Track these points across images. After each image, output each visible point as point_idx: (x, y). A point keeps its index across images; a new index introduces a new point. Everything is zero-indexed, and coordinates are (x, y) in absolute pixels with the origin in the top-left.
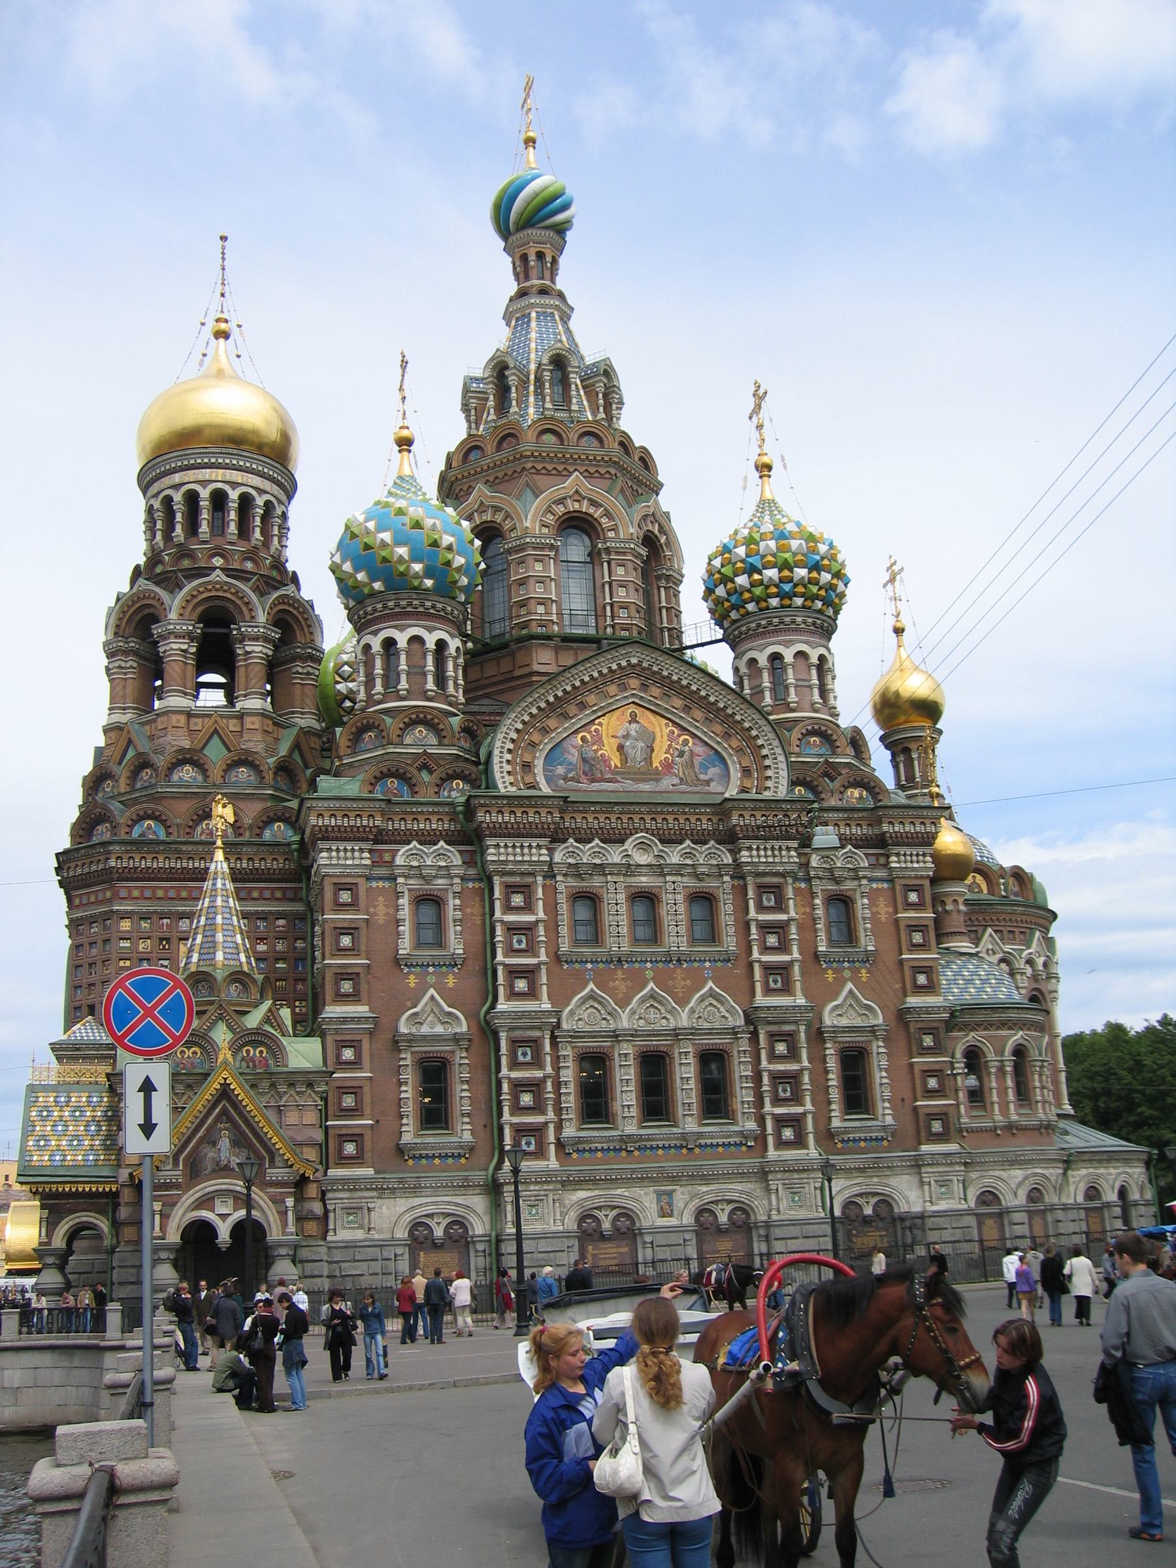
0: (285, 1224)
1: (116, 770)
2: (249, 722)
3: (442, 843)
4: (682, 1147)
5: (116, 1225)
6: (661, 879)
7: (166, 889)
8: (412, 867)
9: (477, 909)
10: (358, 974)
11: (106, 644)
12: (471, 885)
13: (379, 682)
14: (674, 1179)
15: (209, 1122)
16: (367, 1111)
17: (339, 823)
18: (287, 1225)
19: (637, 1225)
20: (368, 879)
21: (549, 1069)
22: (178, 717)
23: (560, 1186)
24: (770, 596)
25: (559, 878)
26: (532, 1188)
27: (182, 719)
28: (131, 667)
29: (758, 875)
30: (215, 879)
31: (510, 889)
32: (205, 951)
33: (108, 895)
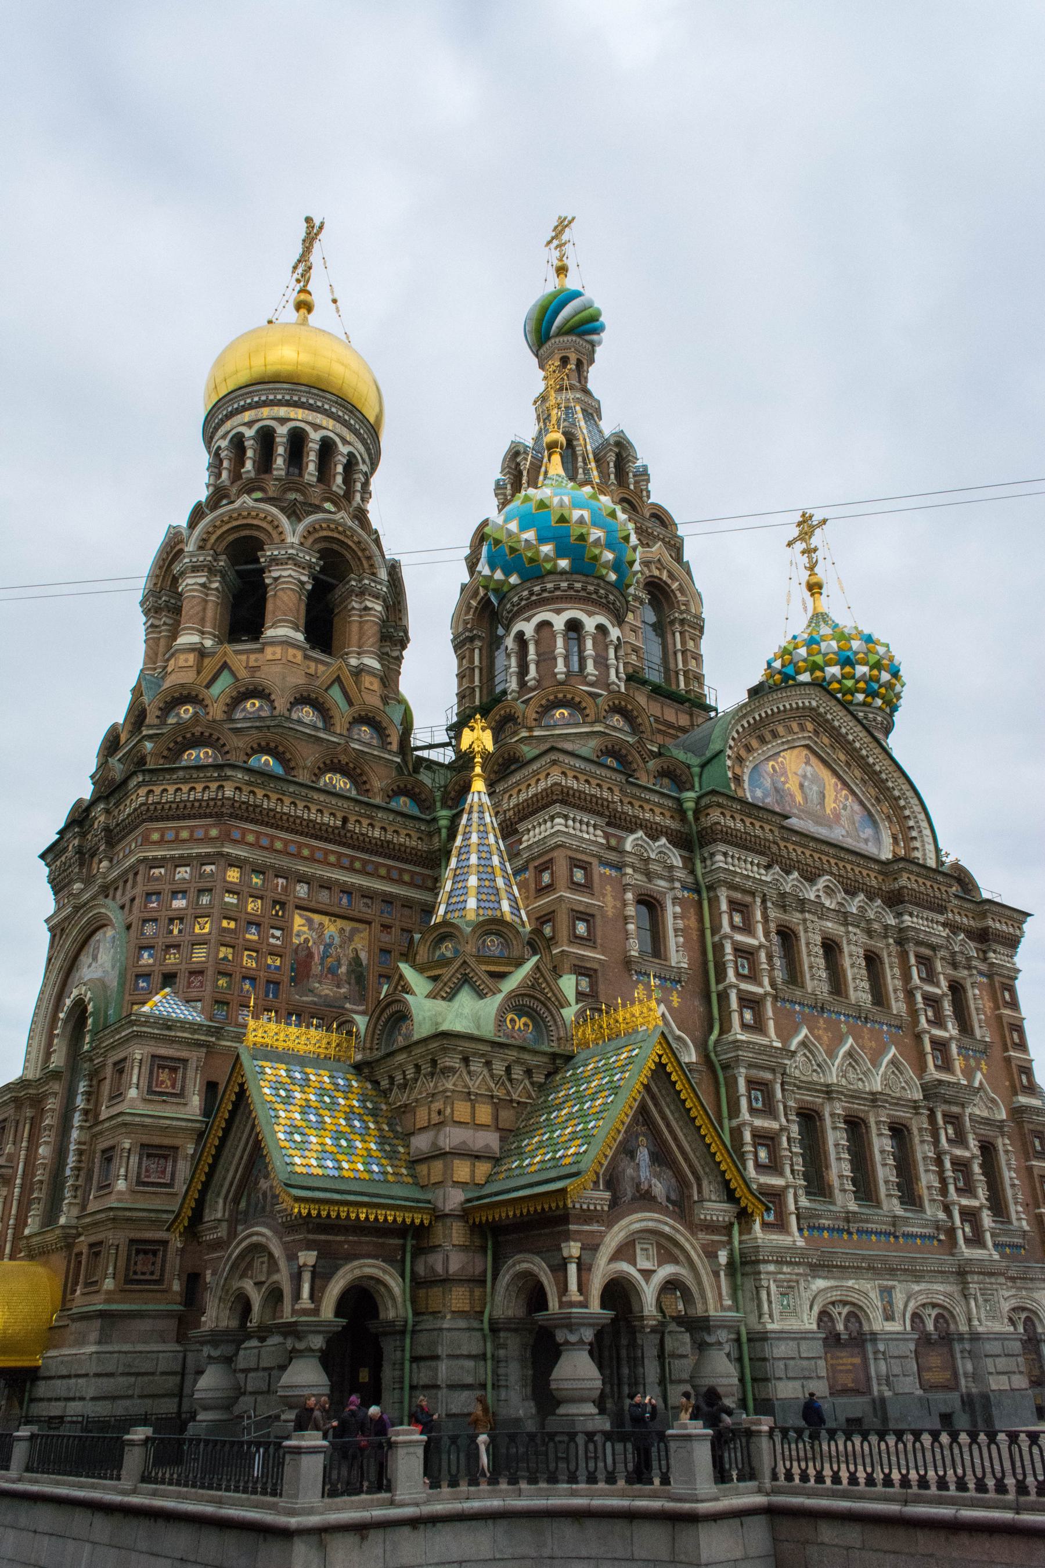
3: (663, 841)
4: (890, 1234)
5: (418, 1284)
6: (842, 929)
7: (286, 842)
9: (693, 923)
10: (595, 971)
12: (686, 894)
13: (560, 662)
14: (892, 1272)
19: (866, 1328)
21: (783, 1120)
23: (808, 1271)
24: (857, 691)
25: (769, 904)
26: (785, 1269)
28: (217, 589)
29: (919, 943)
30: (481, 812)
31: (735, 906)
32: (484, 897)
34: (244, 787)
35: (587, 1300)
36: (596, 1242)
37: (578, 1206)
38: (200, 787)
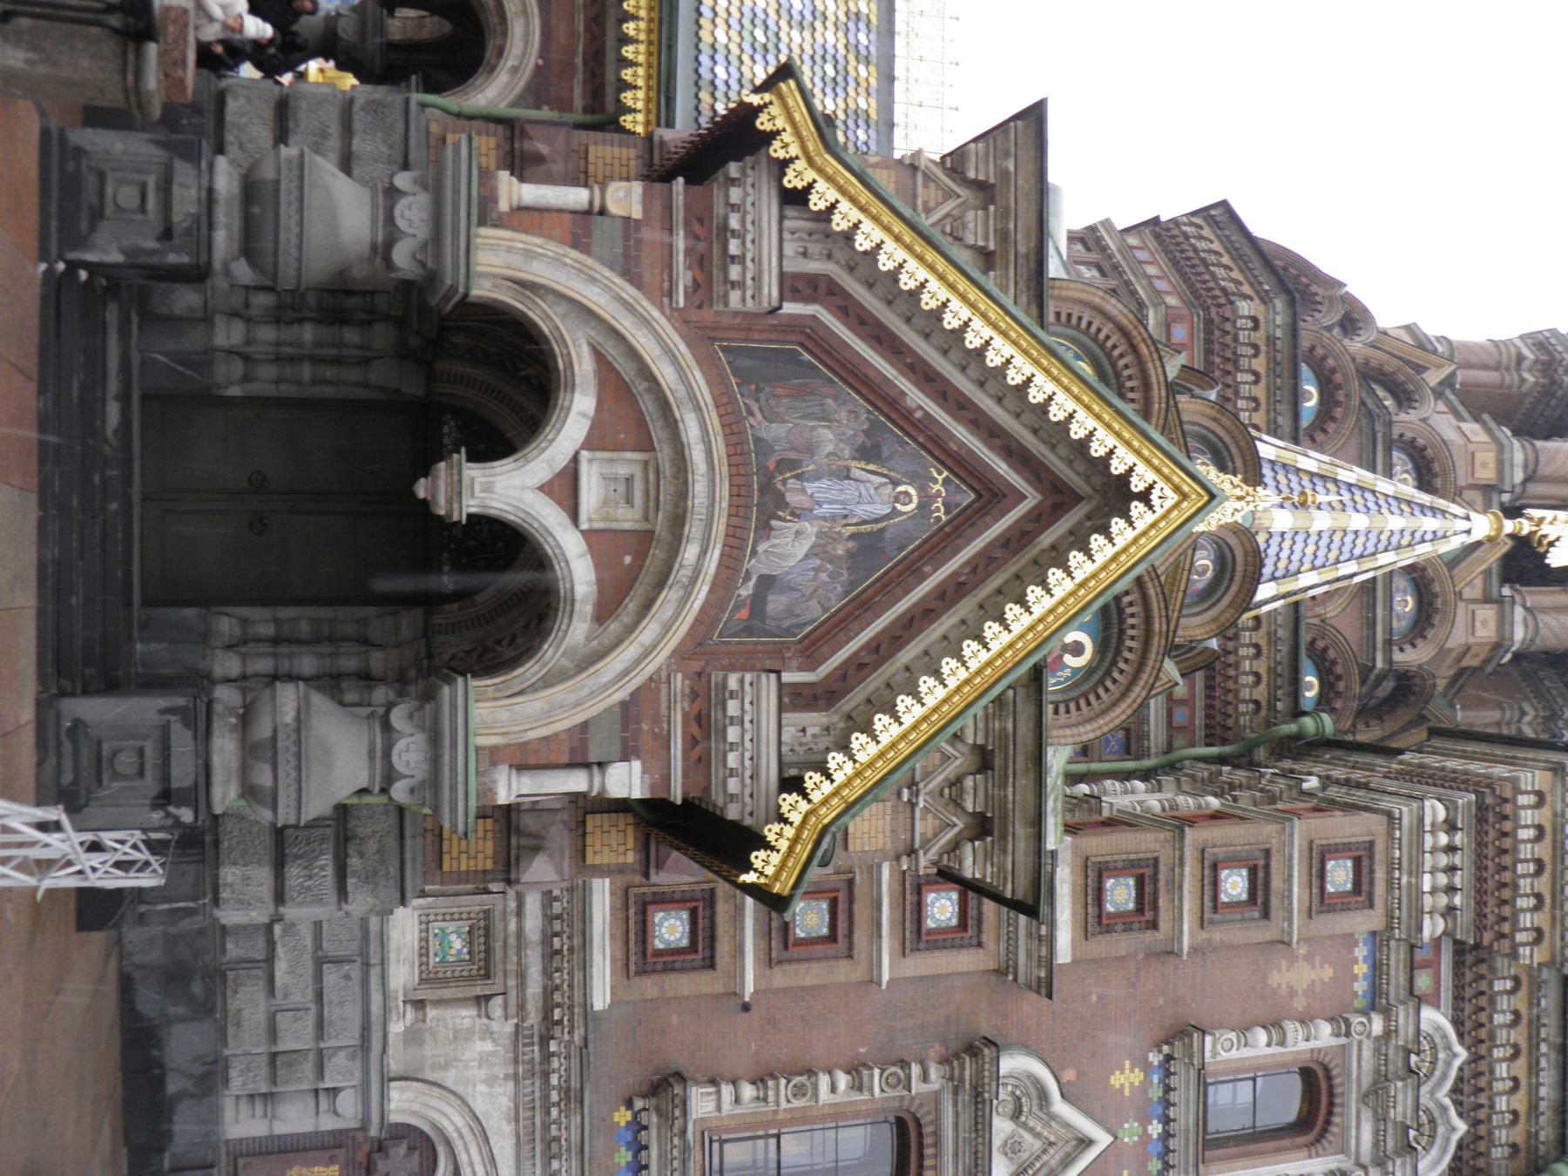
0: (526, 760)
1: (1368, 336)
2: (1487, 613)
3: (1462, 1127)
8: (1408, 1052)
10: (1153, 925)
11: (1554, 332)
15: (961, 433)
16: (781, 977)
17: (1526, 851)
18: (521, 767)
20: (1374, 934)
22: (1492, 465)
27: (1487, 474)
28: (1523, 380)
30: (1434, 511)
33: (1172, 301)
34: (1261, 333)
35: (499, 223)
36: (647, 277)
37: (735, 194)
38: (1236, 274)
